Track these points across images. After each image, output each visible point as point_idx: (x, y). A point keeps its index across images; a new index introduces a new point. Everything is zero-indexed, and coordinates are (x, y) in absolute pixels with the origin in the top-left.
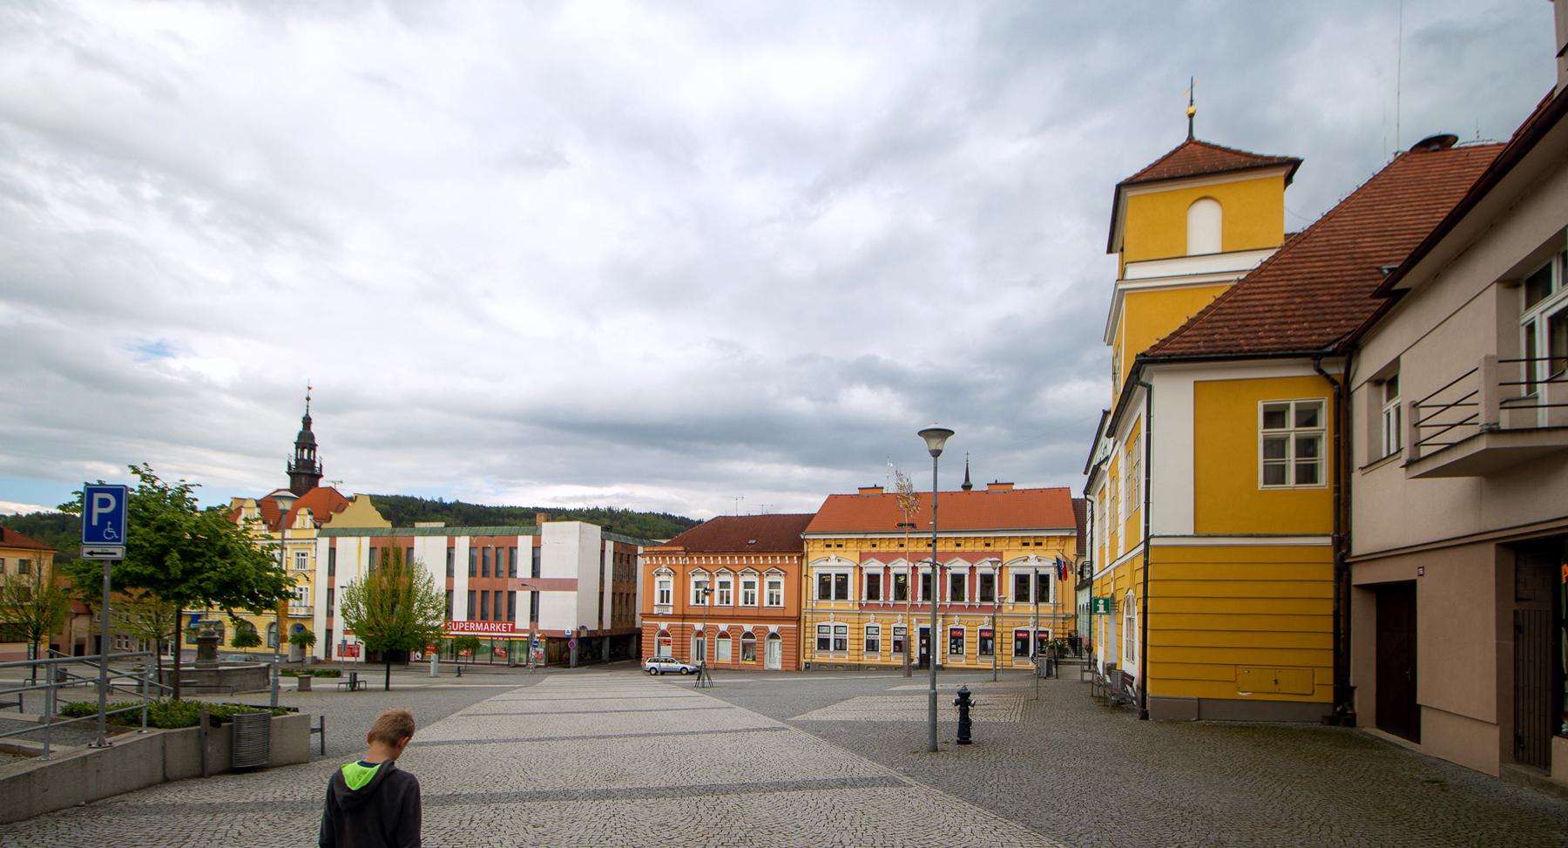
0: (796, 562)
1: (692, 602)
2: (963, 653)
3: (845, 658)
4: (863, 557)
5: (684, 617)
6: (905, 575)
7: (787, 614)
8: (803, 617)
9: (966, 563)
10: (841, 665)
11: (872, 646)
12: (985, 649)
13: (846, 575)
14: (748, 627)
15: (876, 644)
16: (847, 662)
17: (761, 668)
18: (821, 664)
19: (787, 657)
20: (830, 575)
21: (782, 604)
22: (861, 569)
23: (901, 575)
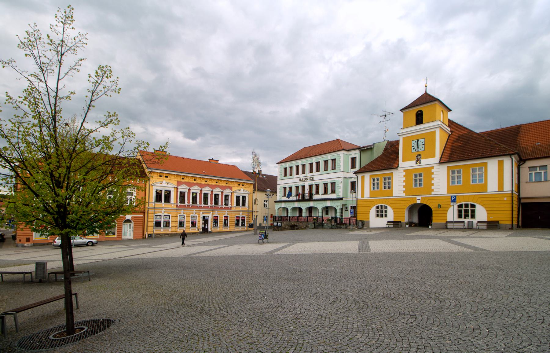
2: (217, 226)
3: (169, 231)
4: (179, 183)
6: (196, 193)
10: (168, 234)
11: (181, 224)
12: (226, 225)
15: (182, 223)
16: (170, 232)
17: (120, 239)
18: (157, 234)
20: (162, 191)
22: (177, 188)
23: (194, 193)
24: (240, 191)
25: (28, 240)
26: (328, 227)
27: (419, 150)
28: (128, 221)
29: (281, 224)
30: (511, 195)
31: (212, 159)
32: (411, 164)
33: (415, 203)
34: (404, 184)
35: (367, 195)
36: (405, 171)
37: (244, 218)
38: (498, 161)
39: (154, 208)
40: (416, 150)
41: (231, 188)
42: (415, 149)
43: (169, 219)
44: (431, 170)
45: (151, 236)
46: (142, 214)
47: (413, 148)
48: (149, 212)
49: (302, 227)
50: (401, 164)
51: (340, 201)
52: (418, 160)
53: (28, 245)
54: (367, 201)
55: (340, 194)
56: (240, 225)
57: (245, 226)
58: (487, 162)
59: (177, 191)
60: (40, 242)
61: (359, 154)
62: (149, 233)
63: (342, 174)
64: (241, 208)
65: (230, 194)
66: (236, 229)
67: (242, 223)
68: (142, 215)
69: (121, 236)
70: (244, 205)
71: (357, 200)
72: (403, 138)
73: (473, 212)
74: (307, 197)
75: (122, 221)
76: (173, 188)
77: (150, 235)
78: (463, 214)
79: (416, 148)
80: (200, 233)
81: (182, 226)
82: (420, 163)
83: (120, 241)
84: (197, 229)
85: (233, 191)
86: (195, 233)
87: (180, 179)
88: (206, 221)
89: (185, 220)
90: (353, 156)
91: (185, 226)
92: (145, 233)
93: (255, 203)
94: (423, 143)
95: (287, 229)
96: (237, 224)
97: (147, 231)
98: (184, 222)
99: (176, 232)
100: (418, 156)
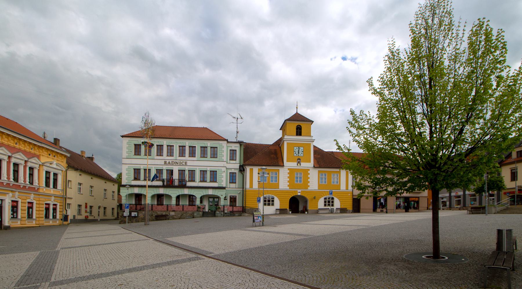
27: (299, 155)
29: (138, 214)
30: (352, 193)
32: (293, 165)
33: (297, 195)
34: (288, 179)
35: (256, 186)
36: (289, 169)
38: (318, 171)
40: (297, 155)
42: (296, 154)
47: (295, 152)
51: (224, 190)
52: (299, 163)
55: (222, 183)
56: (51, 217)
57: (58, 217)
63: (225, 164)
64: (51, 191)
66: (46, 223)
70: (55, 186)
73: (333, 202)
74: (176, 183)
78: (327, 203)
79: (297, 153)
82: (300, 165)
90: (233, 148)
93: (68, 186)
94: (303, 151)
96: (47, 216)
100: (298, 159)
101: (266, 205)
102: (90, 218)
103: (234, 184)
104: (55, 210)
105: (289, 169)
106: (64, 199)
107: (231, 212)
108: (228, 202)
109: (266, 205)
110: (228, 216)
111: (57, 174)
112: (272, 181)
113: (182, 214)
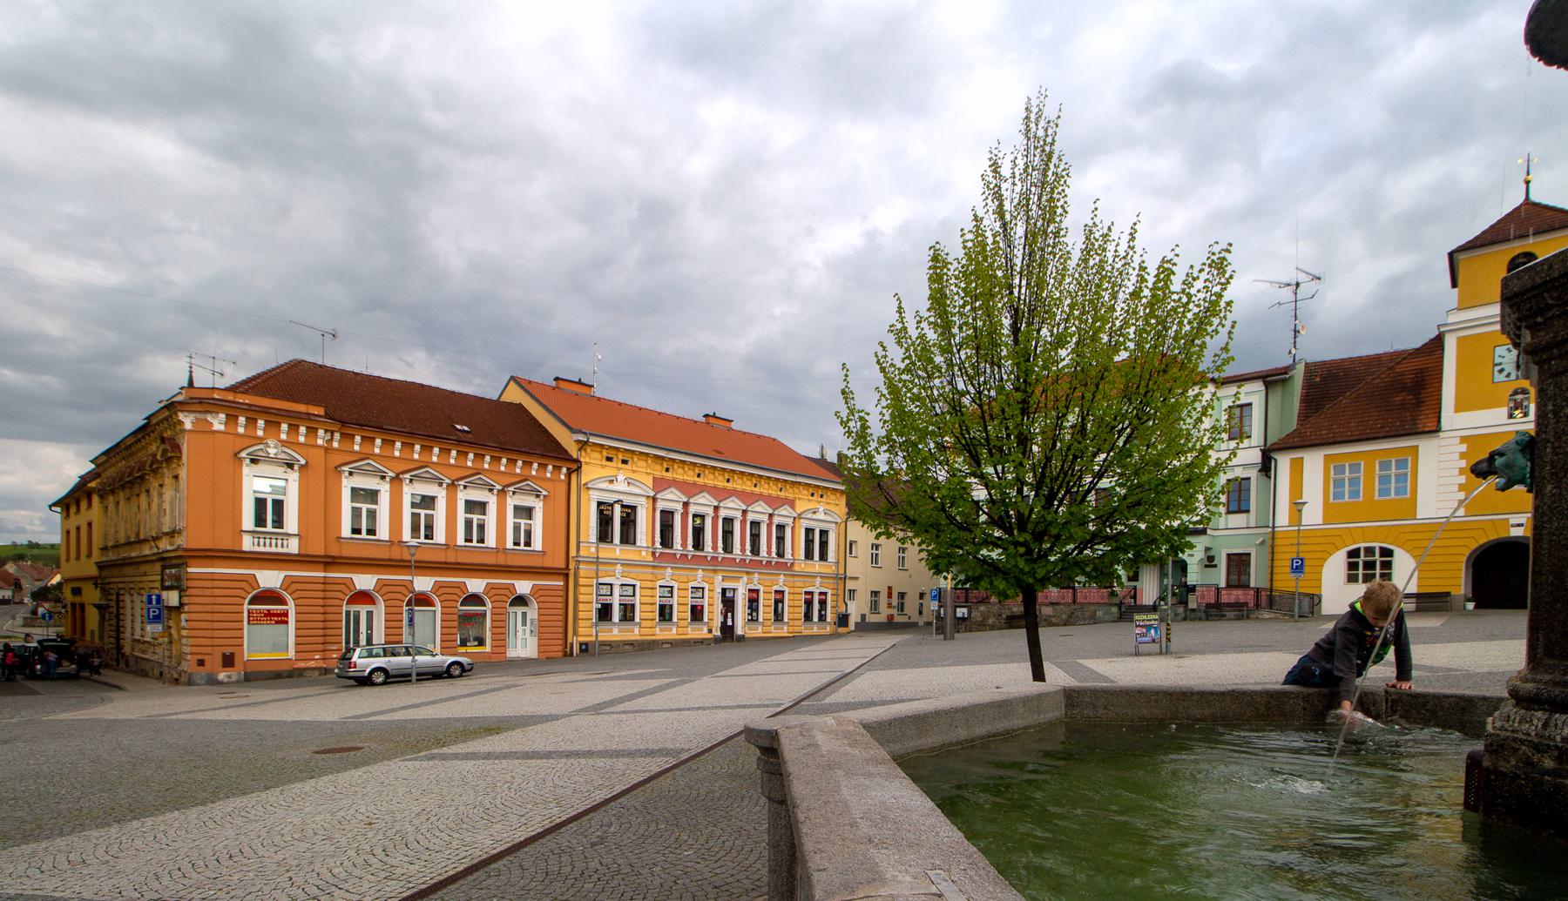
0: (563, 477)
1: (346, 531)
2: (757, 620)
3: (634, 633)
4: (660, 484)
5: (330, 562)
6: (703, 517)
7: (548, 563)
8: (572, 566)
9: (713, 500)
10: (631, 643)
11: (665, 613)
12: (778, 616)
13: (634, 508)
14: (476, 585)
15: (667, 611)
16: (639, 638)
18: (603, 644)
19: (547, 636)
21: (537, 544)
22: (654, 499)
24: (814, 513)
25: (228, 661)
26: (1176, 615)
28: (520, 601)
29: (969, 613)
31: (714, 416)
35: (1313, 515)
36: (1463, 439)
37: (823, 597)
39: (597, 561)
41: (792, 503)
42: (1505, 373)
43: (634, 595)
44: (1468, 448)
45: (586, 650)
46: (562, 577)
47: (1497, 368)
48: (582, 573)
49: (1054, 620)
50: (1450, 417)
53: (229, 677)
54: (1314, 533)
56: (816, 618)
58: (1417, 446)
59: (654, 509)
60: (265, 668)
61: (1263, 393)
62: (581, 639)
64: (816, 566)
65: (790, 521)
66: (806, 630)
67: (820, 611)
68: (562, 583)
69: (502, 650)
70: (823, 557)
71: (1273, 532)
72: (1459, 338)
75: (505, 598)
76: (644, 499)
77: (584, 647)
80: (716, 640)
81: (667, 617)
83: (502, 664)
84: (705, 630)
85: (799, 512)
86: (702, 642)
87: (659, 472)
88: (729, 604)
89: (675, 601)
91: (675, 619)
92: (569, 640)
93: (851, 553)
95: (993, 628)
96: (808, 617)
97: (575, 633)
98: (671, 606)
99: (653, 638)
100: (1516, 393)
101: (1357, 581)
102: (898, 619)
103: (1245, 515)
104: (823, 603)
105: (1463, 439)
106: (842, 582)
107: (1209, 606)
108: (1220, 577)
109: (1357, 581)
110: (1200, 619)
111: (827, 532)
112: (1384, 492)
113: (1073, 613)
